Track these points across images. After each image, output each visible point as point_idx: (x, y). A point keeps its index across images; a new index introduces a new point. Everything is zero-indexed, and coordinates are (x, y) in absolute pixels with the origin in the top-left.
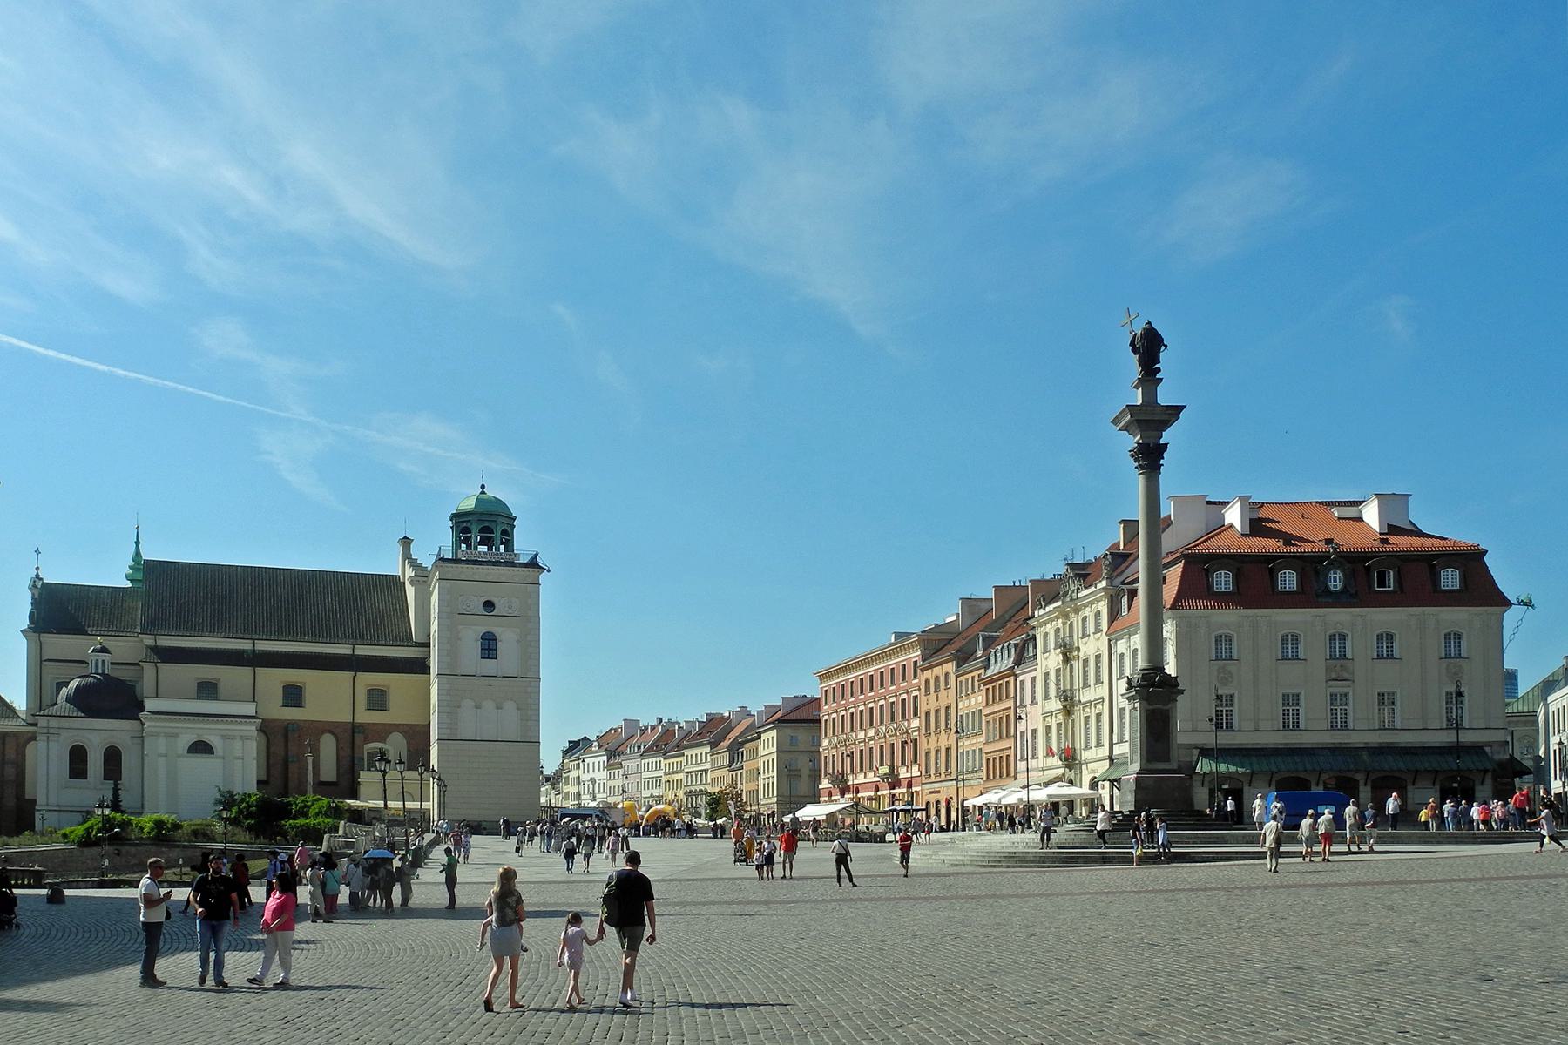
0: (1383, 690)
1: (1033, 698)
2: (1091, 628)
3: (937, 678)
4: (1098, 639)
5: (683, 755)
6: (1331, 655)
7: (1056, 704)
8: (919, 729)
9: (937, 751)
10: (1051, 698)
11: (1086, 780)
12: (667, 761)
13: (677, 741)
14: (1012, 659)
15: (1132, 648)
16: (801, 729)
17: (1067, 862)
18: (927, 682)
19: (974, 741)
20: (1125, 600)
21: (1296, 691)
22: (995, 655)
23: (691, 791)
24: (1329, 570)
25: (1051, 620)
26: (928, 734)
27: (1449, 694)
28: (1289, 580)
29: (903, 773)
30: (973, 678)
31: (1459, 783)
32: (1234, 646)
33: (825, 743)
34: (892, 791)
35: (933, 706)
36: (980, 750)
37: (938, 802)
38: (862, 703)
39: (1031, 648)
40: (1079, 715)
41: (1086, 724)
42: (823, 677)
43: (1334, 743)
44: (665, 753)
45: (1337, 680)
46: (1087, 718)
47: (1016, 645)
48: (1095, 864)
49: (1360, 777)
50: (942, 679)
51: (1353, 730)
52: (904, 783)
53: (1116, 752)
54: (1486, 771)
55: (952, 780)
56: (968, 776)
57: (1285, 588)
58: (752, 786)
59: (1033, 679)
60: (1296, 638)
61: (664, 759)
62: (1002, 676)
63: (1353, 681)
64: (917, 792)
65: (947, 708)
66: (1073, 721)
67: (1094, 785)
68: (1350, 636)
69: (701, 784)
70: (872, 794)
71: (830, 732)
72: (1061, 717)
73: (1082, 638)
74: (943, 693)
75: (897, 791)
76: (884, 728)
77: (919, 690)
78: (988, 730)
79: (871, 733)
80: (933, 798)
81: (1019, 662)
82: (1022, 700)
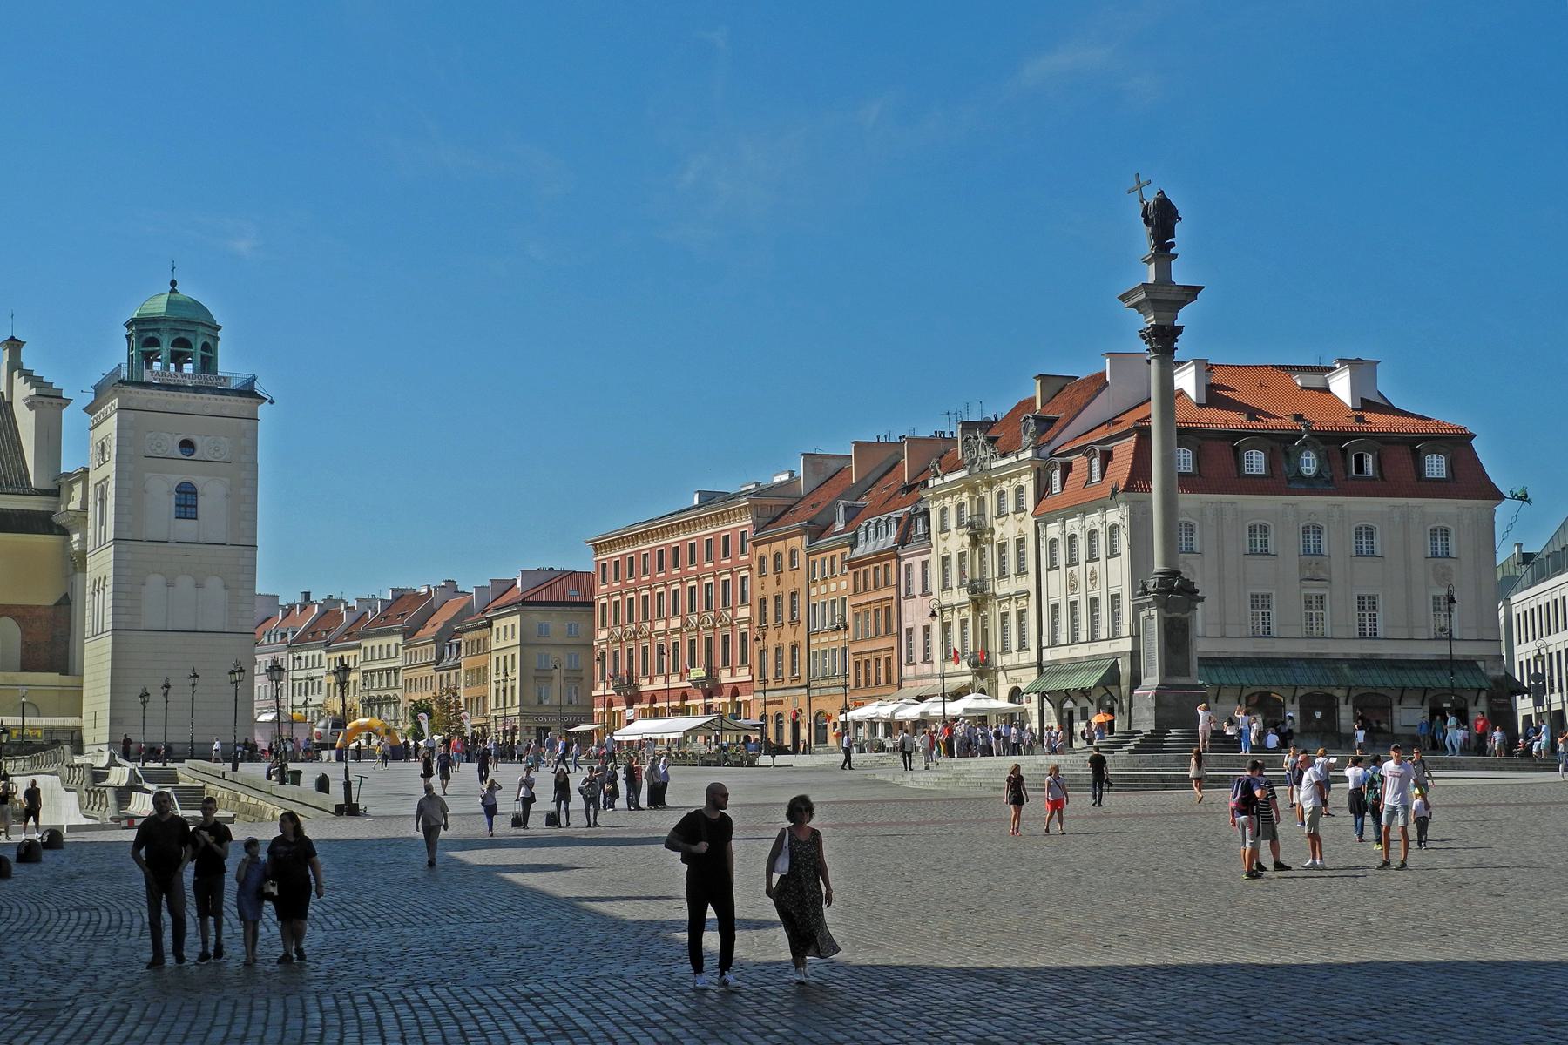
0: (1363, 593)
1: (925, 587)
2: (1010, 506)
3: (777, 556)
4: (1021, 520)
5: (359, 646)
6: (1304, 550)
7: (960, 596)
8: (749, 621)
9: (777, 650)
10: (952, 588)
11: (1004, 689)
12: (332, 656)
13: (346, 626)
14: (893, 537)
15: (1069, 533)
16: (554, 615)
17: (1126, 785)
18: (762, 559)
19: (823, 640)
20: (1057, 476)
21: (1267, 591)
22: (877, 529)
23: (370, 699)
24: (1301, 453)
25: (952, 493)
26: (763, 629)
27: (1436, 599)
28: (1256, 462)
29: (725, 676)
30: (833, 558)
31: (1453, 703)
32: (1196, 537)
33: (603, 635)
34: (707, 701)
35: (771, 589)
36: (845, 649)
37: (779, 716)
38: (658, 584)
39: (920, 525)
40: (994, 612)
41: (1003, 622)
42: (598, 548)
43: (1311, 654)
44: (328, 644)
45: (1312, 580)
46: (1004, 616)
47: (898, 520)
48: (1155, 787)
49: (1340, 694)
50: (786, 557)
51: (1332, 638)
52: (727, 690)
53: (1048, 656)
54: (1480, 690)
55: (801, 687)
56: (817, 683)
57: (1252, 470)
58: (474, 692)
59: (925, 564)
60: (1265, 530)
61: (327, 652)
62: (879, 557)
63: (1330, 582)
64: (747, 703)
65: (793, 595)
66: (985, 617)
67: (1015, 694)
68: (1325, 529)
69: (388, 688)
70: (677, 704)
71: (610, 621)
72: (967, 613)
73: (996, 518)
74: (787, 576)
75: (716, 700)
76: (696, 618)
77: (750, 569)
78: (856, 625)
79: (676, 623)
80: (772, 710)
81: (903, 540)
82: (908, 590)
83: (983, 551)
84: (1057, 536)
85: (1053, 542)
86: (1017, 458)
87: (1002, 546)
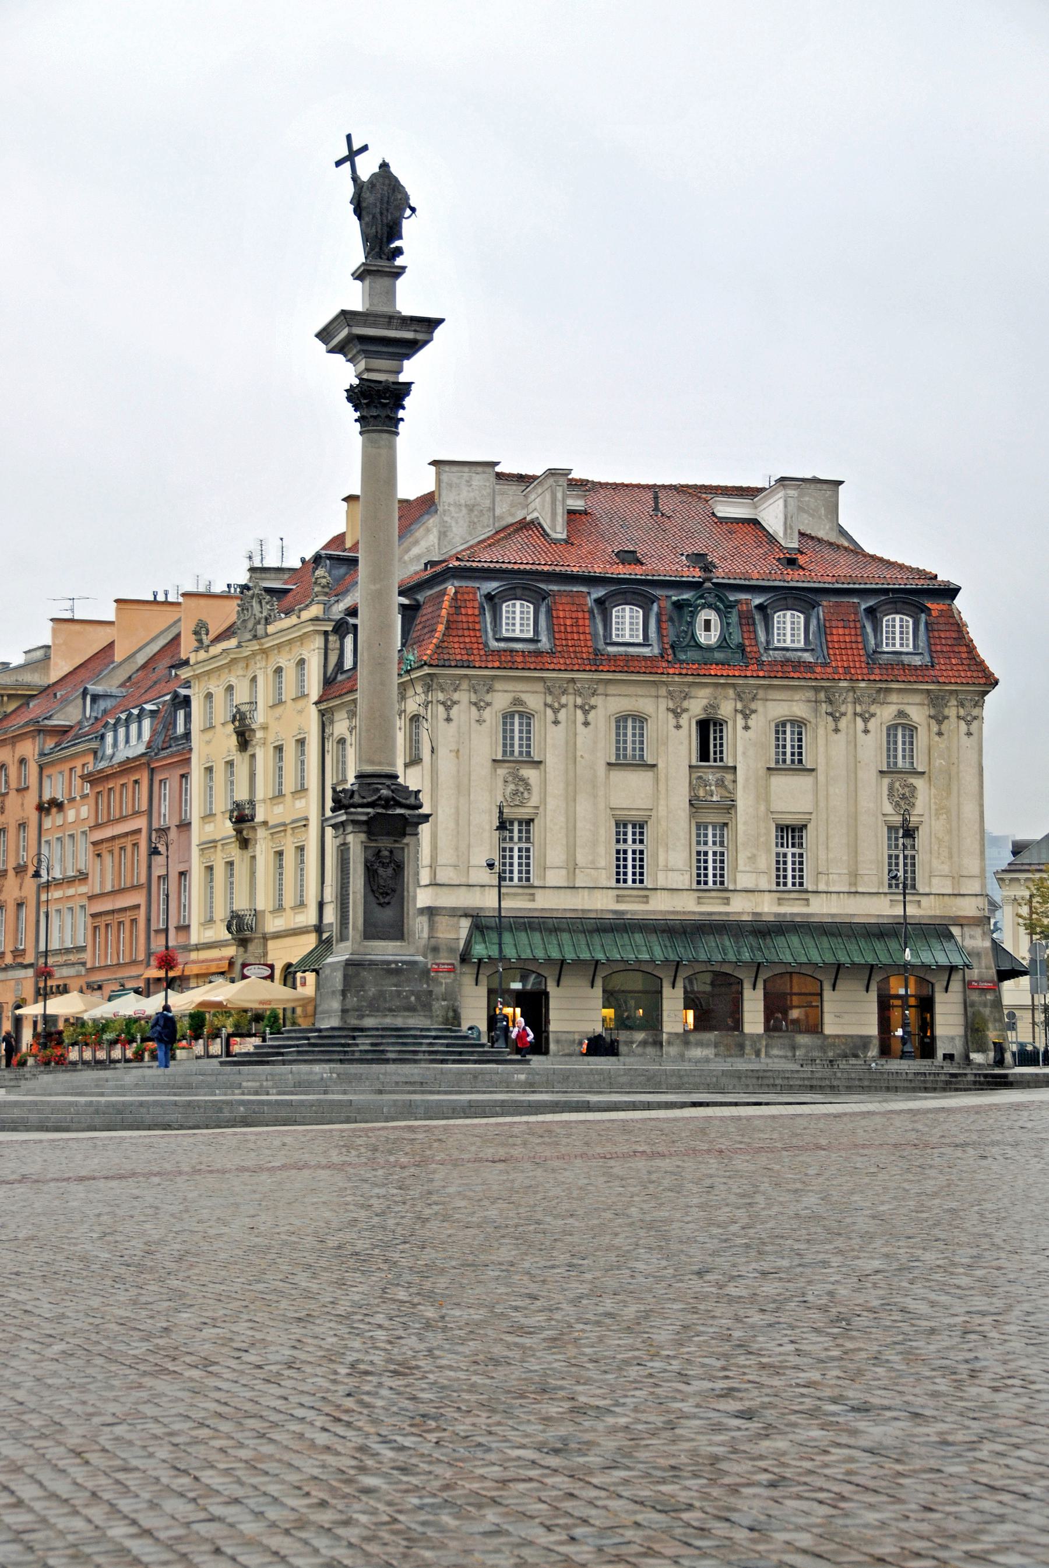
83: (253, 756)
84: (347, 735)
85: (342, 741)
86: (299, 617)
87: (279, 749)
